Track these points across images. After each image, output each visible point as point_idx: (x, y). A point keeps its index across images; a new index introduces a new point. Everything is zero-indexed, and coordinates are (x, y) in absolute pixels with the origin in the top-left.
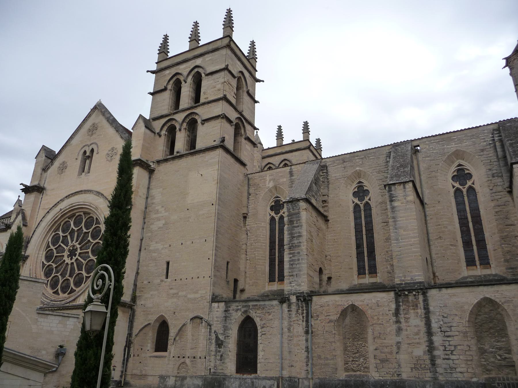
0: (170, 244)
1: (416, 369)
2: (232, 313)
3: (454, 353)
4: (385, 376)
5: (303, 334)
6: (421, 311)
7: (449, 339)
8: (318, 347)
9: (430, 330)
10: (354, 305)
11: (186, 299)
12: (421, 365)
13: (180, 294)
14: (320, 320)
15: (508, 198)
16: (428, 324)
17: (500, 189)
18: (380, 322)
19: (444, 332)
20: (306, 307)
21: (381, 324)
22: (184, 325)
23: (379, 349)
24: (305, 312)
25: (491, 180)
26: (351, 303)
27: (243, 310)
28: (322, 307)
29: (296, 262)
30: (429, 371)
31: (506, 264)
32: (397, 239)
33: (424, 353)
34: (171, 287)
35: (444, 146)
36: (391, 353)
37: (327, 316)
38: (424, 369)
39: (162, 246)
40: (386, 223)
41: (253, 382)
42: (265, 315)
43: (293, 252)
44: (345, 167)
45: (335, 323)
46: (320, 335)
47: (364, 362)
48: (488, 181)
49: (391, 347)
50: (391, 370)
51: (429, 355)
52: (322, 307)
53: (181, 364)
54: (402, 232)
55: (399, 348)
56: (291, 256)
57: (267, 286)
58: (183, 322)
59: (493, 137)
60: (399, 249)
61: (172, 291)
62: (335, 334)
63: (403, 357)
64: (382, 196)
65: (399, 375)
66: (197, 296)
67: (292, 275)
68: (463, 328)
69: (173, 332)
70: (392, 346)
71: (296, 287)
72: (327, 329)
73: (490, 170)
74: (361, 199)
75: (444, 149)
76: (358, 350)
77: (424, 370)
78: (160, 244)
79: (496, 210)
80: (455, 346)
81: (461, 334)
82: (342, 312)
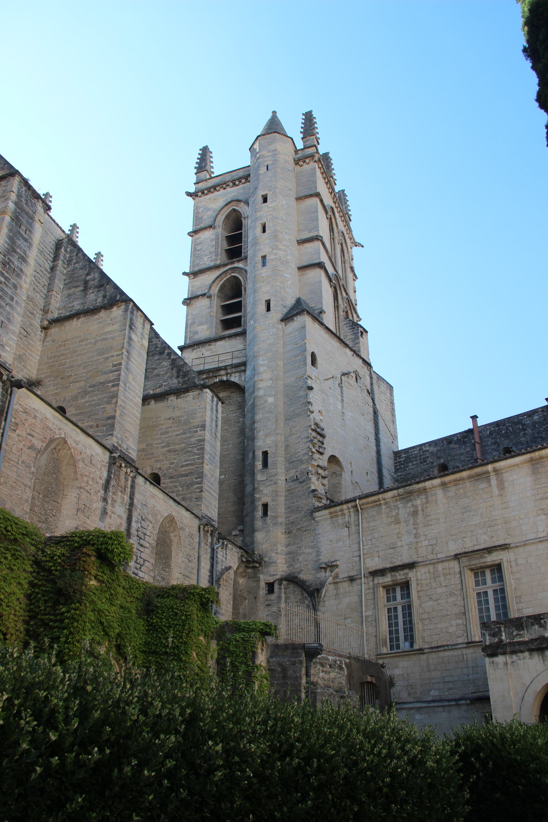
6: (127, 498)
7: (142, 549)
10: (66, 442)
14: (18, 435)
18: (88, 488)
26: (64, 436)
28: (26, 412)
32: (125, 385)
37: (30, 435)
40: (26, 333)
43: (8, 276)
45: (37, 455)
46: (12, 463)
52: (26, 412)
54: (131, 377)
62: (33, 473)
72: (24, 457)
76: (46, 518)
80: (144, 561)
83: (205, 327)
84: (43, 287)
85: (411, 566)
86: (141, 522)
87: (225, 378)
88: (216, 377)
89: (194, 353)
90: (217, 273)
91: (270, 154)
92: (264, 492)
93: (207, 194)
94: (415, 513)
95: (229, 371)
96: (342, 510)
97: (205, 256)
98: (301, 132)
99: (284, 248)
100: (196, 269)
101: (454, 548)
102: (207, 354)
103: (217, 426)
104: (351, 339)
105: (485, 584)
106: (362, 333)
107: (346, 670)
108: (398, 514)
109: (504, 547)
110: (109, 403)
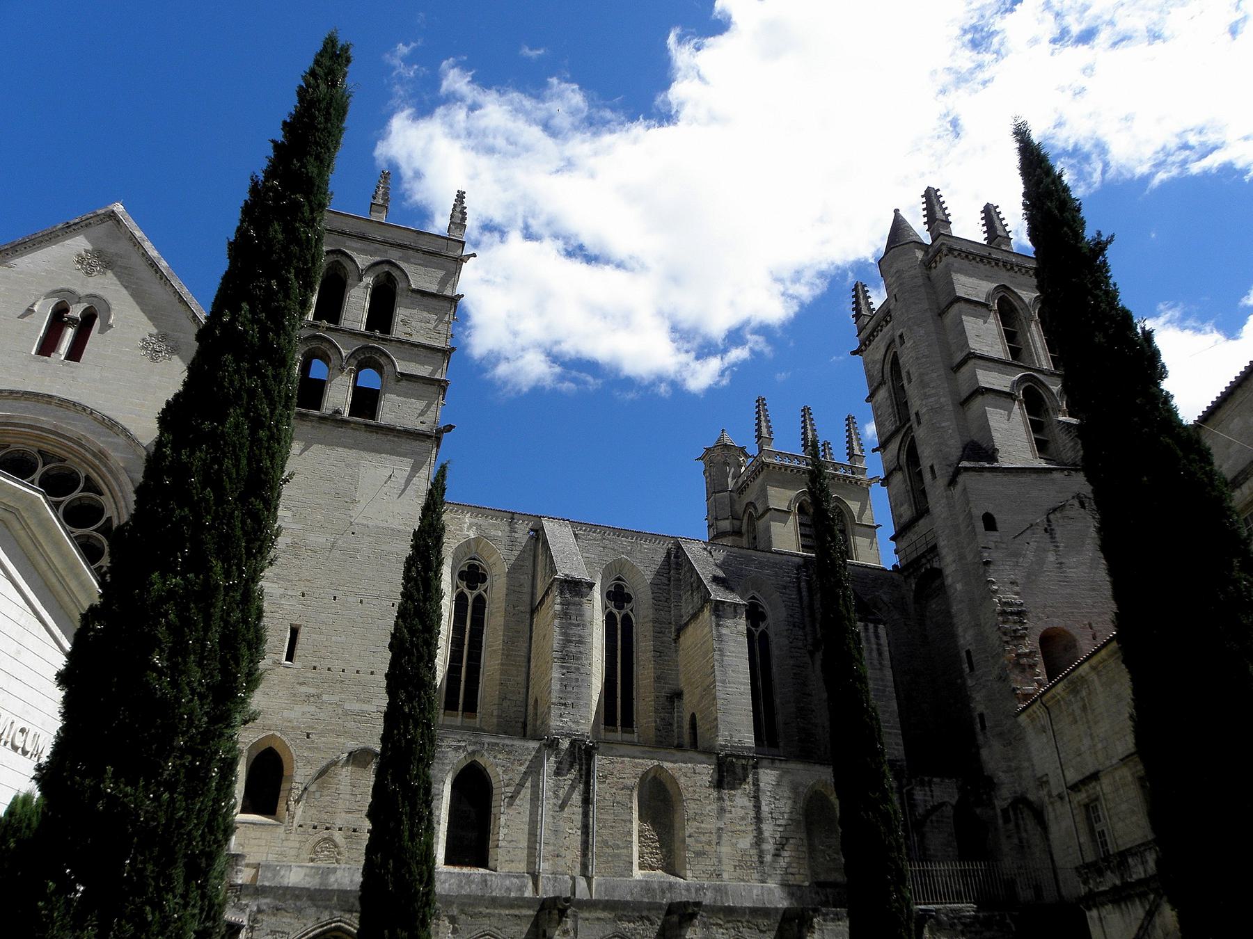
0: (304, 589)
2: (447, 752)
3: (786, 848)
5: (580, 804)
8: (605, 827)
11: (340, 712)
13: (325, 697)
16: (757, 807)
17: (800, 644)
19: (776, 819)
20: (587, 760)
21: (698, 800)
22: (334, 763)
24: (584, 768)
27: (470, 748)
29: (573, 684)
34: (302, 680)
36: (709, 843)
38: (750, 867)
39: (282, 591)
41: (486, 881)
42: (512, 764)
44: (604, 547)
50: (709, 868)
53: (319, 842)
55: (720, 837)
56: (565, 671)
57: (442, 716)
58: (331, 756)
59: (798, 574)
60: (724, 696)
61: (303, 689)
63: (725, 849)
66: (366, 707)
67: (565, 705)
69: (300, 773)
71: (569, 724)
72: (618, 799)
74: (620, 607)
77: (750, 869)
78: (275, 585)
79: (794, 671)
82: (643, 775)
83: (906, 506)
85: (1095, 777)
90: (900, 437)
93: (869, 345)
95: (929, 558)
97: (887, 420)
99: (933, 392)
100: (883, 439)
102: (914, 538)
103: (880, 654)
104: (1071, 447)
107: (1012, 925)
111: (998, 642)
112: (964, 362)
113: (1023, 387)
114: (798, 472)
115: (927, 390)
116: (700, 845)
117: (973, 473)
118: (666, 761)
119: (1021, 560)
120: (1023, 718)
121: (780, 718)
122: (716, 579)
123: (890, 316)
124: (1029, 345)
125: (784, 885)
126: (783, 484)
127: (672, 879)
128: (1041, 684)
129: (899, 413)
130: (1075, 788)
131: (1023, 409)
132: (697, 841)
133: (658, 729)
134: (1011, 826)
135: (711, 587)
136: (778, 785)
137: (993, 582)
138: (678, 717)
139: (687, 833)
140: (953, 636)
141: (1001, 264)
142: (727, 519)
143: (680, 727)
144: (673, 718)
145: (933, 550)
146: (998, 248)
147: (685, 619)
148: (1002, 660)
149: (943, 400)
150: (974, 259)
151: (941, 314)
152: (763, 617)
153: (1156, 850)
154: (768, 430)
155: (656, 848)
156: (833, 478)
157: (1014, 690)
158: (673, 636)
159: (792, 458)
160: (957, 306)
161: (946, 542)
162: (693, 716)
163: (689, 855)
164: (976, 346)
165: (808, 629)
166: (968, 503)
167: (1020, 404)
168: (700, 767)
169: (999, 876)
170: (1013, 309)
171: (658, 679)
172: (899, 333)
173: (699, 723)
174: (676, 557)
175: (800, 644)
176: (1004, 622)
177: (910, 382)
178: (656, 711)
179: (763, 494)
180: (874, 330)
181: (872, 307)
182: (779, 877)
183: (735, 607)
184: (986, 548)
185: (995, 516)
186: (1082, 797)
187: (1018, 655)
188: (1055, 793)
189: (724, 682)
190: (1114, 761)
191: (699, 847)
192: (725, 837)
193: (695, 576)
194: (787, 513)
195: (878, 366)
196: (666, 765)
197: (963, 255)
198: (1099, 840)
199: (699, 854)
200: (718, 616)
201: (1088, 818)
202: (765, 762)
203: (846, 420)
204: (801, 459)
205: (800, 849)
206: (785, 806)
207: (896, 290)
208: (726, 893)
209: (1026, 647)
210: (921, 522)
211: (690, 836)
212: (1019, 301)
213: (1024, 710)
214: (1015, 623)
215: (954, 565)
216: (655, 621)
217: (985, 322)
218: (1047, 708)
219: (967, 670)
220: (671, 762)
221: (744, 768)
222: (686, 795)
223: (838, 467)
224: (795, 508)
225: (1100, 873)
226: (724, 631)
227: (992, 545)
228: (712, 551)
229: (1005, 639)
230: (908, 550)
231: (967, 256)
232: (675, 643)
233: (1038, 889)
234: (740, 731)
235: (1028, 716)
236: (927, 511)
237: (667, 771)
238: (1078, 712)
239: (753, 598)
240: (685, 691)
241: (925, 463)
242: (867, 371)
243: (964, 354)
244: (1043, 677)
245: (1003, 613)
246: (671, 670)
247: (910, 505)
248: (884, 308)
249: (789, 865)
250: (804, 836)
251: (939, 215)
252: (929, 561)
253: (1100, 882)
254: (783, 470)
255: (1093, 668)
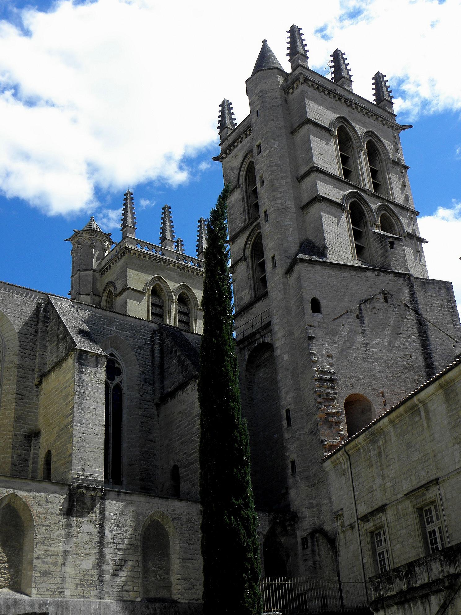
1: (82, 585)
3: (123, 569)
4: (45, 593)
9: (103, 540)
12: (88, 580)
15: (154, 411)
16: (102, 533)
17: (149, 397)
18: (47, 523)
19: (117, 544)
21: (48, 526)
23: (41, 558)
25: (143, 385)
30: (95, 589)
31: (141, 482)
33: (93, 566)
35: (104, 324)
36: (55, 564)
38: (91, 586)
40: (21, 396)
47: (15, 576)
48: (140, 385)
49: (57, 557)
50: (53, 586)
51: (97, 569)
55: (65, 559)
60: (81, 435)
63: (69, 570)
64: (22, 357)
65: (62, 592)
68: (135, 542)
70: (58, 555)
73: (143, 373)
75: (103, 329)
77: (90, 587)
79: (142, 420)
81: (133, 548)
83: (246, 291)
84: (32, 350)
85: (382, 509)
86: (117, 530)
87: (261, 341)
88: (255, 341)
89: (242, 320)
90: (247, 233)
91: (258, 97)
92: (291, 449)
94: (379, 455)
95: (262, 334)
96: (338, 459)
97: (238, 218)
98: (287, 55)
99: (281, 195)
101: (406, 487)
102: (251, 317)
104: (382, 253)
105: (432, 522)
106: (392, 245)
108: (370, 457)
109: (436, 482)
110: (69, 442)
111: (313, 403)
112: (307, 174)
113: (350, 201)
114: (155, 259)
115: (275, 193)
116: (47, 566)
117: (307, 264)
118: (21, 490)
119: (337, 338)
120: (328, 464)
121: (125, 460)
122: (81, 332)
123: (250, 130)
124: (357, 169)
125: (121, 599)
126: (141, 269)
127: (18, 596)
128: (342, 439)
129: (249, 213)
130: (365, 518)
131: (348, 219)
132: (43, 562)
133: (13, 464)
134: (308, 551)
135: (77, 338)
136: (122, 514)
137: (314, 354)
138: (34, 454)
139: (35, 555)
140: (276, 399)
141: (343, 100)
142: (89, 294)
143: (35, 463)
144: (30, 454)
145: (267, 326)
146: (342, 86)
147: (49, 367)
148: (314, 418)
149: (288, 203)
150: (323, 91)
151: (293, 132)
152: (119, 372)
153: (440, 560)
154: (133, 221)
155: (5, 568)
156: (184, 269)
157: (322, 441)
158: (36, 381)
159: (151, 247)
160: (307, 127)
161: (278, 320)
162: (49, 453)
163: (36, 574)
164: (319, 161)
165: (157, 385)
166: (300, 288)
167: (347, 215)
168: (53, 497)
169: (295, 591)
170: (349, 139)
171: (18, 419)
172: (257, 144)
173: (54, 459)
174: (45, 311)
175: (149, 397)
176: (320, 387)
177: (262, 185)
178: (14, 448)
179: (123, 274)
180: (235, 141)
181: (235, 122)
182: (115, 594)
183: (97, 358)
184: (311, 326)
185: (321, 302)
186: (370, 525)
187: (328, 414)
188: (347, 523)
189: (81, 422)
190: (399, 496)
191: (45, 567)
192: (70, 559)
193: (61, 329)
194: (143, 293)
195: (235, 172)
196: (21, 493)
197: (316, 86)
198: (378, 560)
199: (45, 574)
200: (81, 364)
201: (373, 543)
202: (112, 495)
203: (199, 222)
204: (158, 250)
205: (136, 569)
206: (128, 533)
207: (259, 107)
208: (67, 608)
209: (335, 408)
210: (258, 305)
211: (38, 558)
212: (353, 133)
213: (329, 457)
214: (328, 388)
215: (284, 339)
216: (20, 367)
217: (327, 144)
218: (348, 455)
219: (285, 425)
220: (26, 491)
221: (93, 499)
222: (37, 521)
223: (189, 260)
224: (149, 290)
225: (390, 581)
226: (85, 377)
227: (316, 324)
228: (79, 309)
229: (319, 400)
230: (245, 328)
231: (318, 88)
232: (37, 388)
233: (324, 601)
234: (91, 466)
235: (332, 462)
236: (266, 295)
237: (21, 499)
238: (373, 458)
239: (111, 354)
240: (43, 431)
241: (268, 254)
242: (225, 176)
243: (309, 167)
244: (345, 433)
245: (320, 379)
246: (30, 412)
247: (250, 290)
248: (245, 123)
249: (125, 583)
250: (140, 558)
251: (300, 49)
252: (262, 336)
253: (389, 588)
254: (142, 256)
255: (391, 422)
